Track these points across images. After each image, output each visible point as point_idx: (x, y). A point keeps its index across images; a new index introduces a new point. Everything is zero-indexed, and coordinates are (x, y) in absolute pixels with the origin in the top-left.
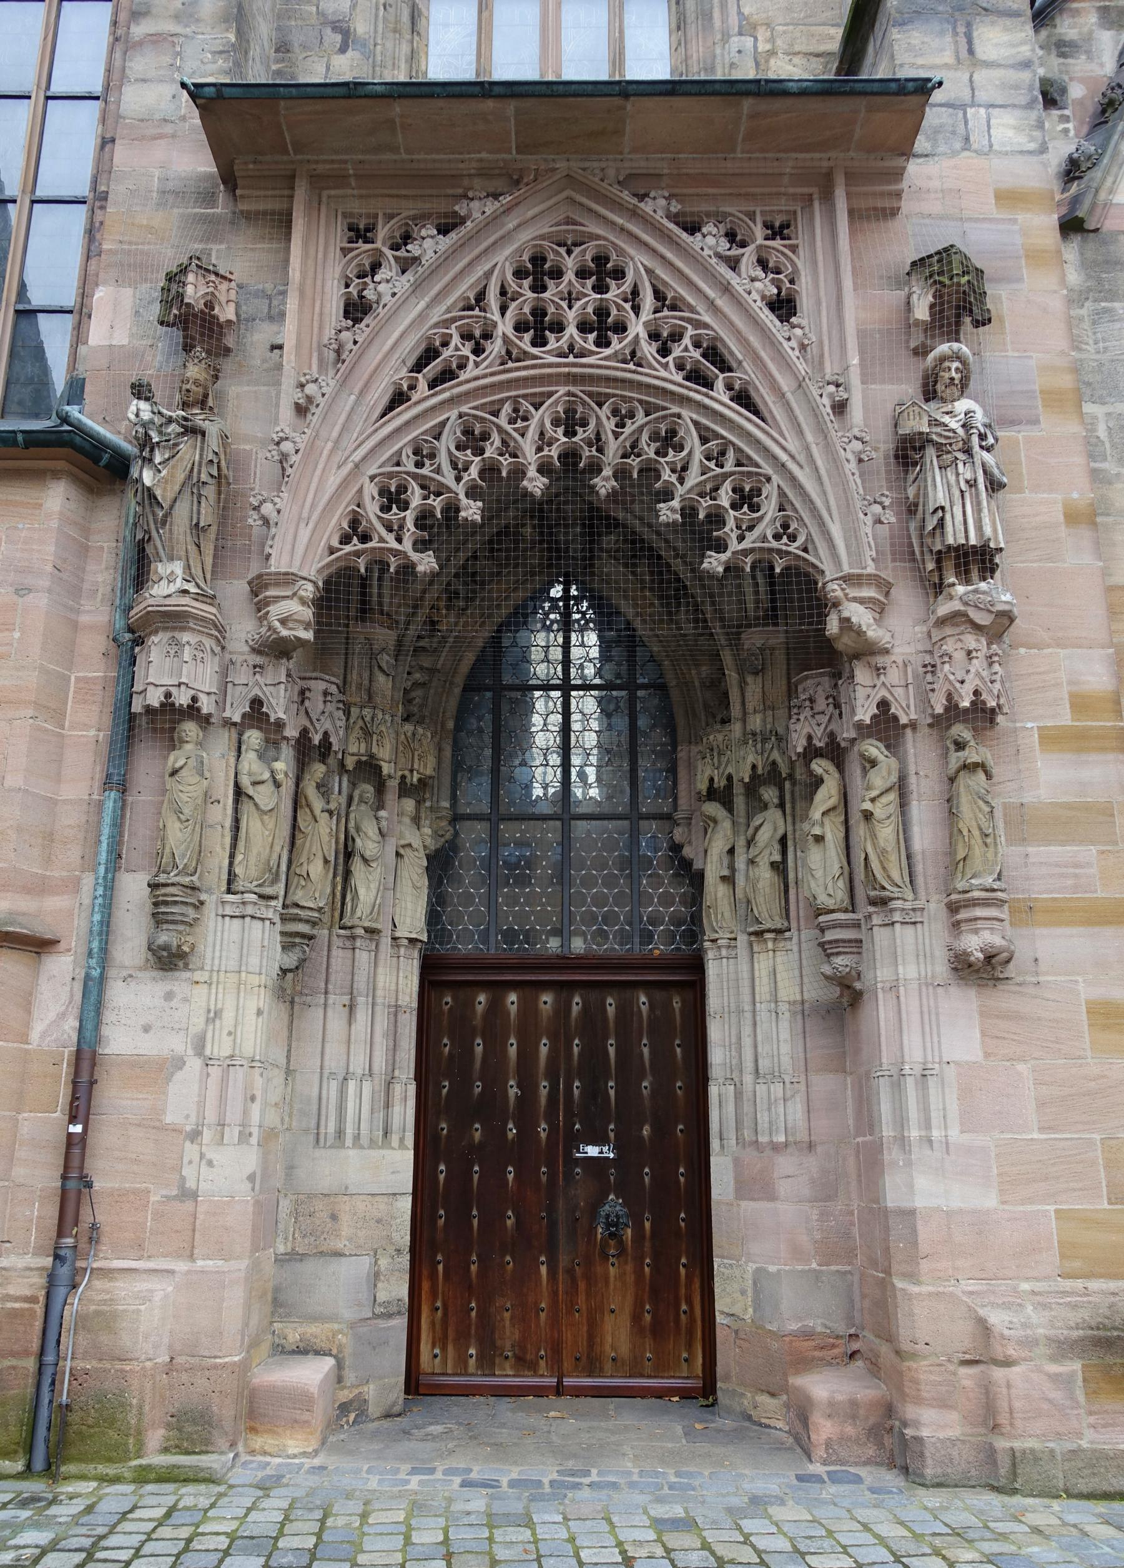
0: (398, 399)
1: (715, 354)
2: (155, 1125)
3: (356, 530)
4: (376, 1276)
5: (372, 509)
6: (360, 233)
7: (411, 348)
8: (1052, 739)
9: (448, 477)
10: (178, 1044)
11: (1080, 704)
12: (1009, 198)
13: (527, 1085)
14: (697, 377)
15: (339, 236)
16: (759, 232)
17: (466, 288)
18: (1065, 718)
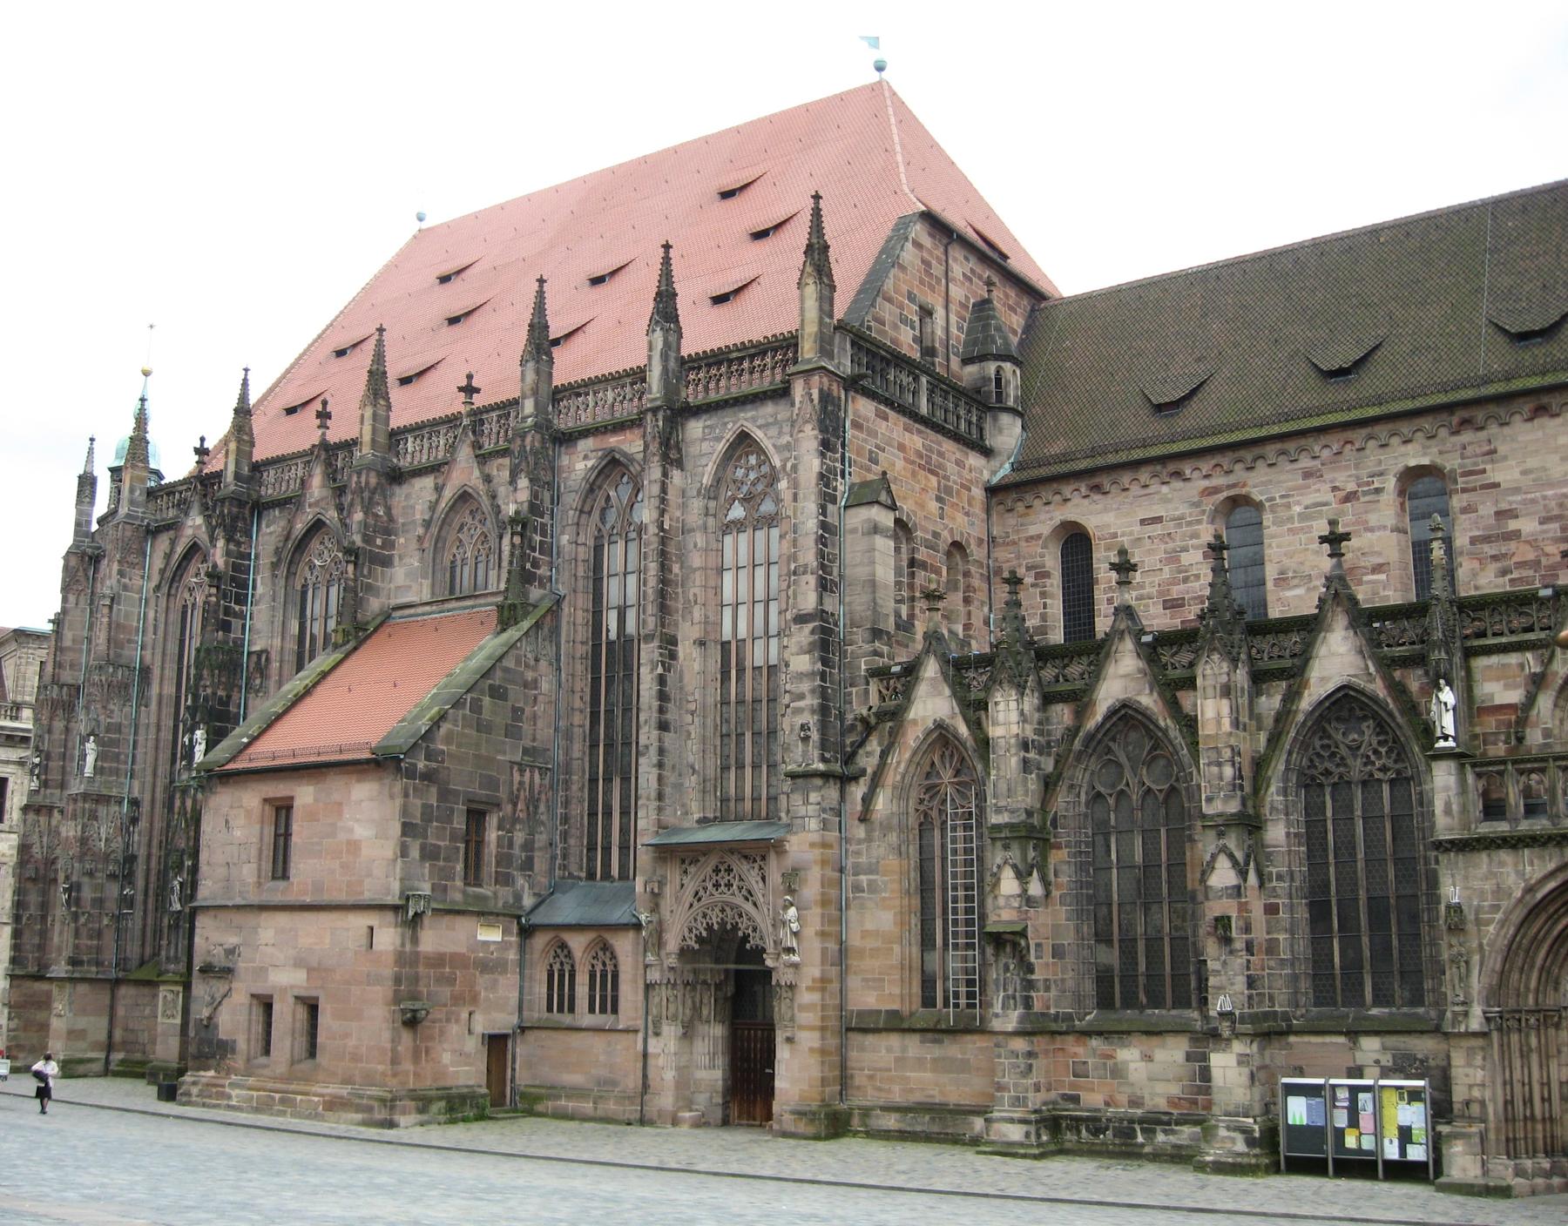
0: (691, 905)
1: (750, 892)
2: (657, 1066)
3: (684, 939)
4: (711, 1098)
5: (687, 935)
6: (683, 862)
7: (693, 893)
8: (809, 989)
9: (699, 926)
10: (659, 1051)
11: (814, 980)
12: (812, 845)
13: (755, 1055)
14: (747, 899)
15: (678, 862)
16: (758, 859)
17: (702, 877)
18: (810, 984)
